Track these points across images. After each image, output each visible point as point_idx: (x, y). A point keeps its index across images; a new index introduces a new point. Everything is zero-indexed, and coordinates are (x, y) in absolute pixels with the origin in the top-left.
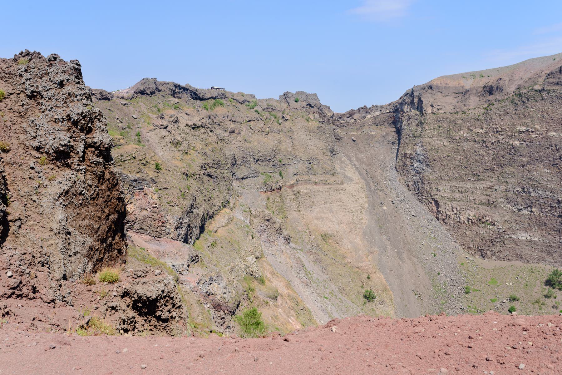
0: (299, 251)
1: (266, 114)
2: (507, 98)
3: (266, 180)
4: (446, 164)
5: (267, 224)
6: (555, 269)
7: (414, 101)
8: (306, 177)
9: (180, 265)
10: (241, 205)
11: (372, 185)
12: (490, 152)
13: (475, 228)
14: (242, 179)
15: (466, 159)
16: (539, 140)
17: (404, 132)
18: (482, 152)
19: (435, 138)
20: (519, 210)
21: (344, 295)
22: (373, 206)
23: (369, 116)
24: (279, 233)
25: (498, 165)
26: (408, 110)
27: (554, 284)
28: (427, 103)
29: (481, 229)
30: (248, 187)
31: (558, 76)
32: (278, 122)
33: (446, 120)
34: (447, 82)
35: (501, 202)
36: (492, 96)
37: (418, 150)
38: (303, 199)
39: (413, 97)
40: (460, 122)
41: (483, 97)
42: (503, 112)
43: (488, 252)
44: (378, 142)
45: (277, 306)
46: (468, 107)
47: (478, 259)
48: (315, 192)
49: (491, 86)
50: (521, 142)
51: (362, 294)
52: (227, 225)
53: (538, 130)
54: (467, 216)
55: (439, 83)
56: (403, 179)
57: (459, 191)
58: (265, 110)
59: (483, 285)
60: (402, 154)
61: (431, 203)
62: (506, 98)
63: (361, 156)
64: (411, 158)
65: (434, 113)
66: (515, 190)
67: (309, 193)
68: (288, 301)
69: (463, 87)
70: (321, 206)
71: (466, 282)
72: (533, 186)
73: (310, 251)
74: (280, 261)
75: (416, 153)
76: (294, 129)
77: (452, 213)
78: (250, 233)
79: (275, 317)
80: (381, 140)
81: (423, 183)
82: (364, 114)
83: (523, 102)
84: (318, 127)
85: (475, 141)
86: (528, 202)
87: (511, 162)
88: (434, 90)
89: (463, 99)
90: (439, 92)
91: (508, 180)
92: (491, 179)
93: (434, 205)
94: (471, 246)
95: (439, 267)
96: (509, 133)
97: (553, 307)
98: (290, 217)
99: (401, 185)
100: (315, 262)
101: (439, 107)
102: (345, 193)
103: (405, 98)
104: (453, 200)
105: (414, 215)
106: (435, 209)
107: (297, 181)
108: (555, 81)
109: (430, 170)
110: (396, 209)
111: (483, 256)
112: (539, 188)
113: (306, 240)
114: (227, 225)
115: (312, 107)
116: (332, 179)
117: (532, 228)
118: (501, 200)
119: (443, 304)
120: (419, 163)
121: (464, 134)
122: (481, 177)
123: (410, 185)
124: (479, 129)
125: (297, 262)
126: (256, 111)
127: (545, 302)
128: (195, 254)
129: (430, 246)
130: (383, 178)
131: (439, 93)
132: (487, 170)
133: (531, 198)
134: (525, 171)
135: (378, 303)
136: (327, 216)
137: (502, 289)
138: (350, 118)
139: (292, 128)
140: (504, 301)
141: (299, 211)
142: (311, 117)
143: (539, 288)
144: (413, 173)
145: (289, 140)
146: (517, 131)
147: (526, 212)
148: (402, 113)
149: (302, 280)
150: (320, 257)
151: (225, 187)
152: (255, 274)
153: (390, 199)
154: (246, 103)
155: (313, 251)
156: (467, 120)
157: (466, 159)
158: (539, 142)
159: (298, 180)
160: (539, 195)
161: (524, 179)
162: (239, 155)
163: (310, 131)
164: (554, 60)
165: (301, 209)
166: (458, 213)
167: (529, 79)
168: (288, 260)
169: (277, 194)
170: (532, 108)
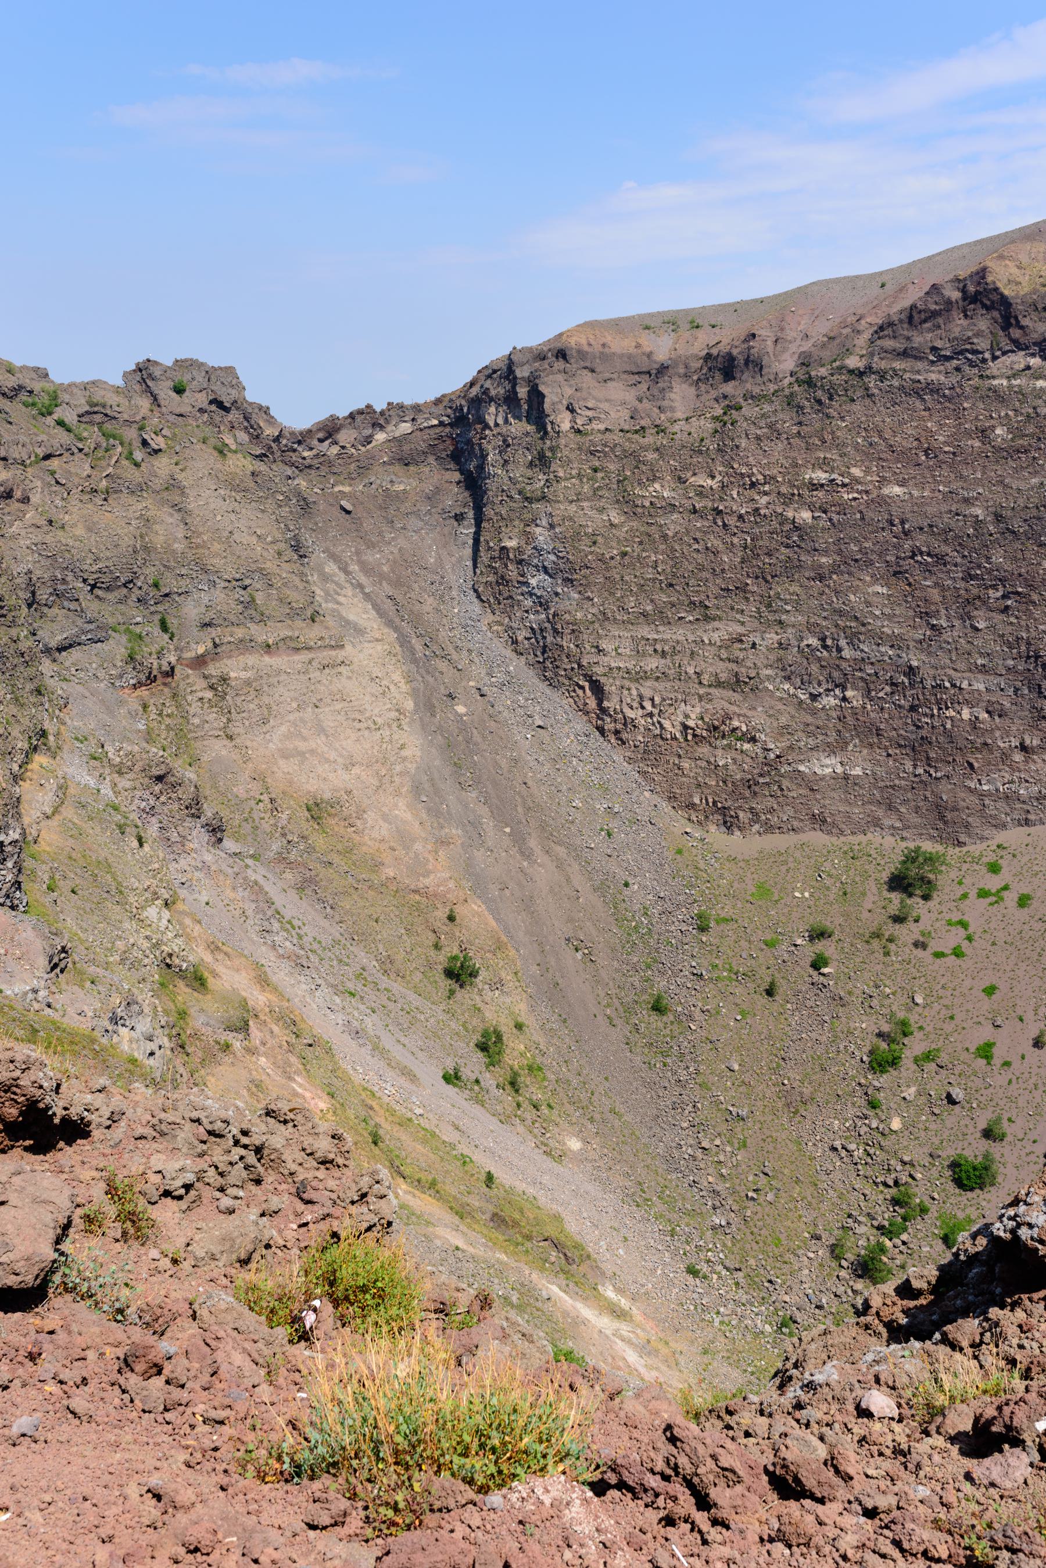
0: (249, 862)
1: (92, 435)
2: (776, 391)
3: (132, 649)
4: (618, 577)
5: (157, 788)
6: (912, 845)
7: (516, 393)
8: (240, 633)
9: (26, 994)
10: (77, 739)
11: (417, 644)
12: (736, 540)
13: (704, 750)
14: (61, 649)
15: (671, 563)
16: (862, 507)
17: (491, 485)
18: (713, 542)
19: (585, 504)
20: (814, 697)
21: (393, 976)
22: (427, 706)
23: (380, 437)
24: (193, 815)
25: (757, 577)
26: (500, 421)
27: (910, 885)
28: (556, 399)
29: (719, 752)
30: (82, 674)
31: (905, 333)
32: (130, 456)
33: (612, 449)
34: (603, 340)
35: (768, 678)
36: (732, 384)
37: (541, 538)
38: (239, 700)
39: (514, 382)
40: (651, 456)
41: (708, 387)
42: (765, 430)
43: (741, 814)
44: (416, 514)
45: (251, 1051)
46: (669, 414)
47: (715, 833)
48: (269, 676)
49: (729, 354)
50: (817, 514)
51: (440, 968)
52: (56, 811)
53: (857, 481)
54: (681, 718)
55: (584, 342)
57: (655, 650)
58: (83, 419)
59: (739, 905)
60: (490, 548)
61: (582, 688)
63: (372, 557)
64: (520, 562)
65: (579, 431)
66: (802, 645)
67: (256, 680)
68: (276, 1029)
69: (649, 355)
70: (291, 717)
71: (695, 901)
72: (848, 631)
73: (281, 859)
74: (206, 899)
75: (535, 548)
76: (185, 479)
77: (640, 712)
78: (128, 830)
79: (257, 1086)
80: (425, 508)
81: (556, 631)
82: (368, 432)
83: (819, 402)
84: (253, 474)
85: (695, 511)
86: (836, 674)
87: (792, 568)
89: (656, 392)
90: (585, 368)
91: (784, 617)
92: (738, 616)
93: (588, 693)
94: (697, 801)
95: (625, 865)
96: (784, 490)
97: (916, 944)
98: (205, 758)
99: (496, 640)
100: (300, 889)
101: (590, 413)
102: (352, 672)
103: (488, 384)
104: (640, 677)
105: (541, 723)
106: (592, 703)
107: (216, 646)
108: (899, 345)
109: (576, 596)
110: (491, 710)
111: (728, 826)
112: (862, 637)
113: (266, 827)
114: (56, 811)
115: (227, 410)
116: (312, 634)
117: (847, 744)
118: (769, 672)
119: (649, 967)
120: (543, 576)
121: (664, 490)
122: (713, 612)
123: (520, 638)
124: (704, 476)
125: (253, 897)
126: (61, 423)
127: (896, 933)
128: (59, 943)
129: (595, 811)
130: (445, 620)
131: (585, 372)
133: (844, 665)
134: (827, 591)
135: (487, 987)
136: (312, 744)
137: (785, 911)
138: (327, 443)
139: (180, 477)
140: (799, 942)
141: (230, 738)
142: (229, 440)
143: (876, 898)
144: (528, 603)
145: (172, 515)
146: (804, 484)
147: (829, 701)
148: (479, 427)
149: (281, 951)
150: (313, 873)
151: (29, 686)
152: (177, 961)
153: (472, 684)
154: (23, 397)
155: (292, 857)
156: (670, 452)
157: (671, 563)
158: (861, 512)
159: (217, 641)
161: (825, 614)
162: (38, 573)
163: (235, 486)
164: (883, 286)
165: (236, 731)
166: (656, 711)
167: (831, 338)
168: (229, 893)
169: (166, 690)
170: (842, 419)
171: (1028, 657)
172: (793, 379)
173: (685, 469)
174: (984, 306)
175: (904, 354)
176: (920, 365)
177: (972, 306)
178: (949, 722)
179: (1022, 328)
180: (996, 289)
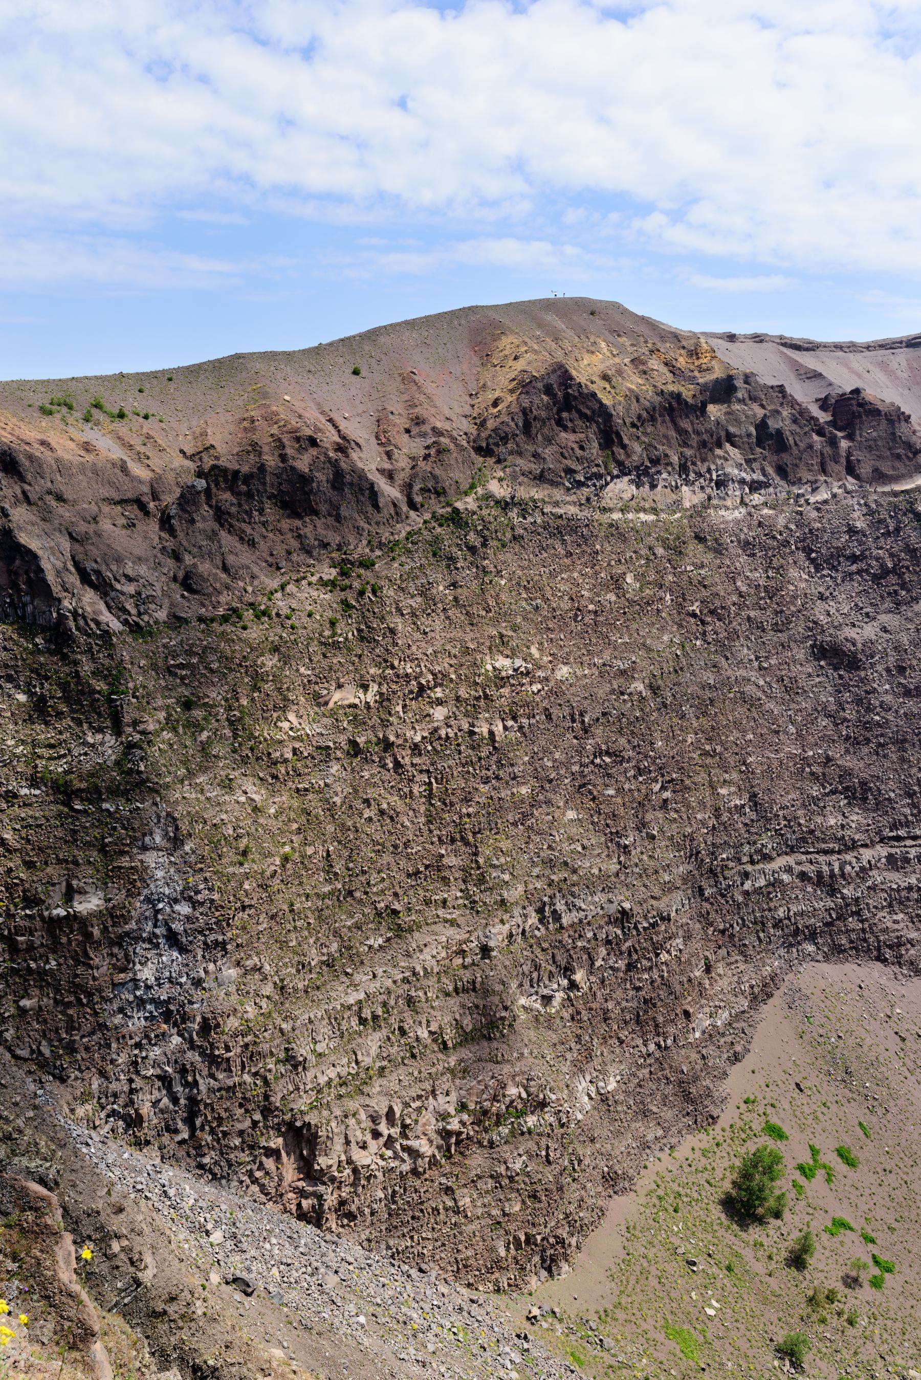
19: (201, 779)
25: (453, 841)
29: (506, 1151)
37: (160, 874)
42: (419, 599)
56: (85, 1098)
57: (363, 1021)
62: (403, 534)
64: (119, 941)
65: (135, 629)
81: (213, 1061)
83: (472, 549)
85: (355, 749)
88: (29, 477)
92: (441, 912)
96: (463, 693)
108: (536, 468)
112: (574, 889)
122: (406, 919)
132: (418, 872)
146: (488, 679)
160: (582, 914)
161: (536, 871)
171: (691, 857)
172: (427, 516)
173: (321, 678)
174: (583, 416)
175: (541, 478)
176: (558, 494)
177: (565, 415)
178: (664, 968)
179: (624, 447)
180: (594, 395)
